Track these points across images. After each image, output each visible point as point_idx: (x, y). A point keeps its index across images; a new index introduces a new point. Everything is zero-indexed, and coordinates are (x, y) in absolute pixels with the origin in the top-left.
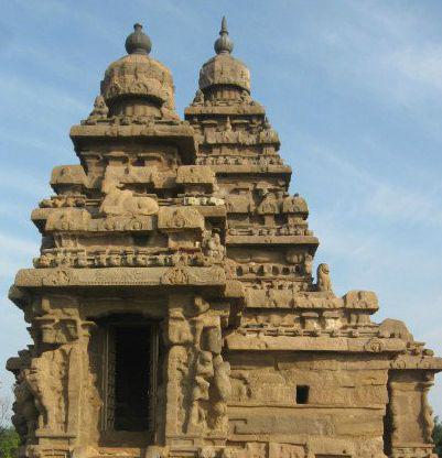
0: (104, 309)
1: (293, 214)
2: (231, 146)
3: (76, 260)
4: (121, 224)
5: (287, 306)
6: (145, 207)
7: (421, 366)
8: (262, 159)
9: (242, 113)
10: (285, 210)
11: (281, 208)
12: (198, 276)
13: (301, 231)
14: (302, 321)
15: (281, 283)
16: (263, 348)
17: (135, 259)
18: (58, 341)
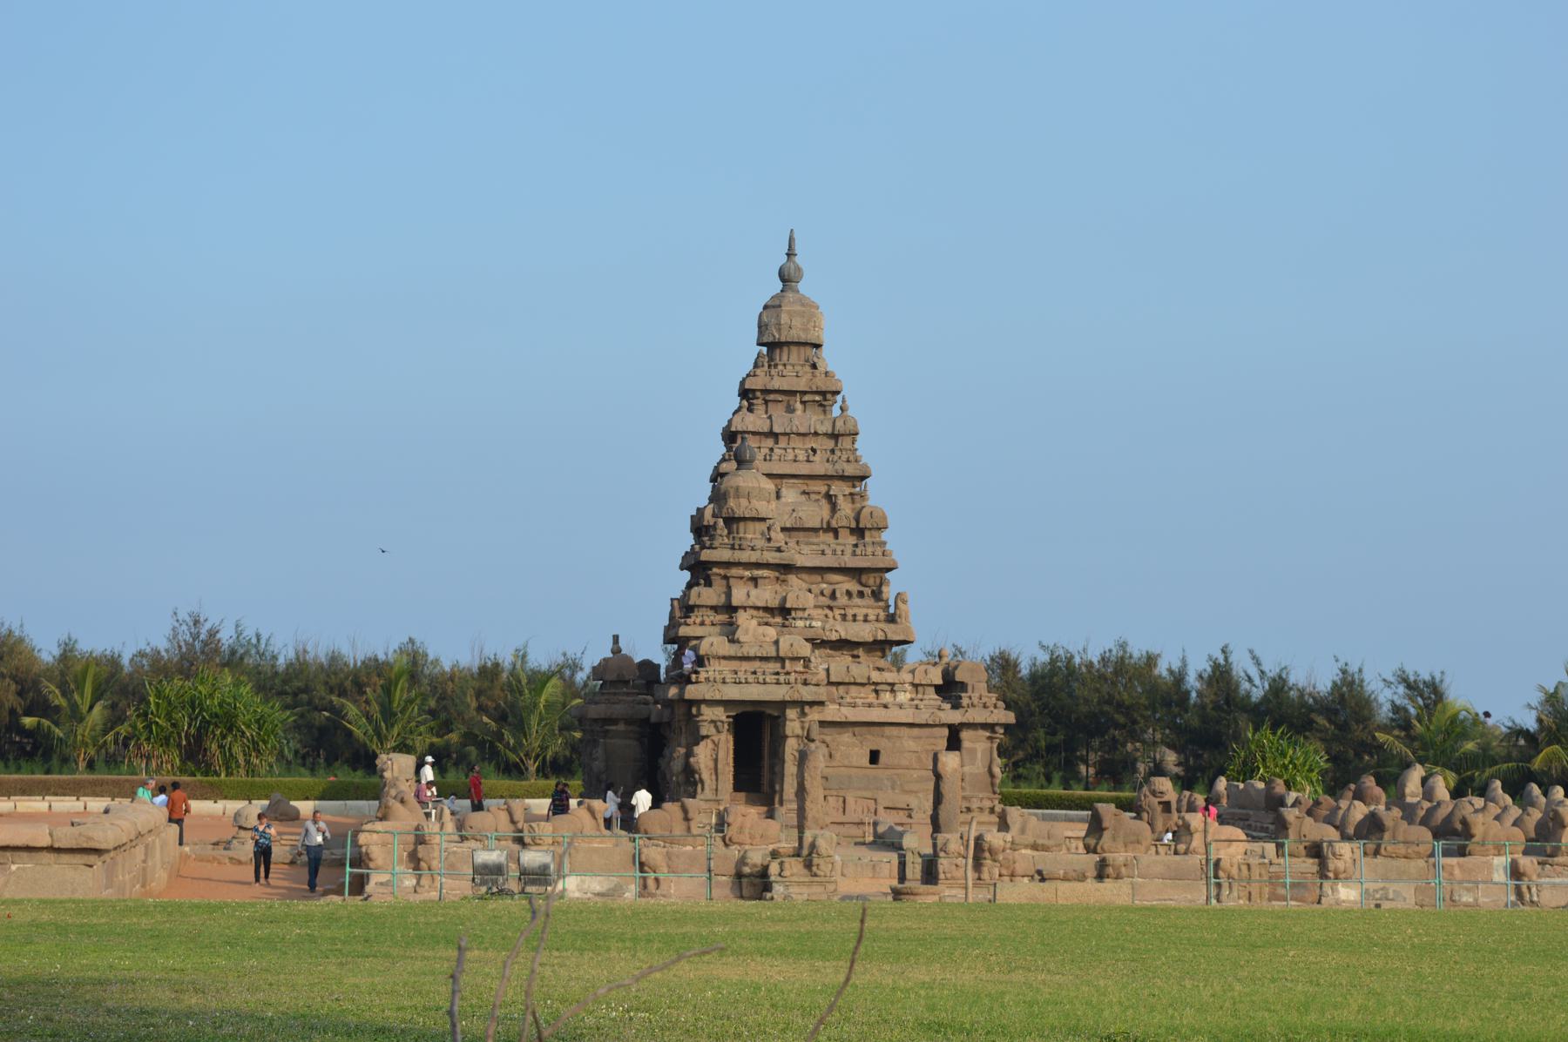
0: (740, 710)
1: (870, 529)
3: (724, 679)
5: (865, 681)
6: (768, 635)
7: (990, 721)
8: (838, 453)
9: (815, 389)
10: (861, 526)
11: (858, 521)
12: (807, 694)
13: (879, 551)
14: (877, 692)
15: (855, 611)
16: (844, 720)
17: (764, 679)
18: (709, 734)
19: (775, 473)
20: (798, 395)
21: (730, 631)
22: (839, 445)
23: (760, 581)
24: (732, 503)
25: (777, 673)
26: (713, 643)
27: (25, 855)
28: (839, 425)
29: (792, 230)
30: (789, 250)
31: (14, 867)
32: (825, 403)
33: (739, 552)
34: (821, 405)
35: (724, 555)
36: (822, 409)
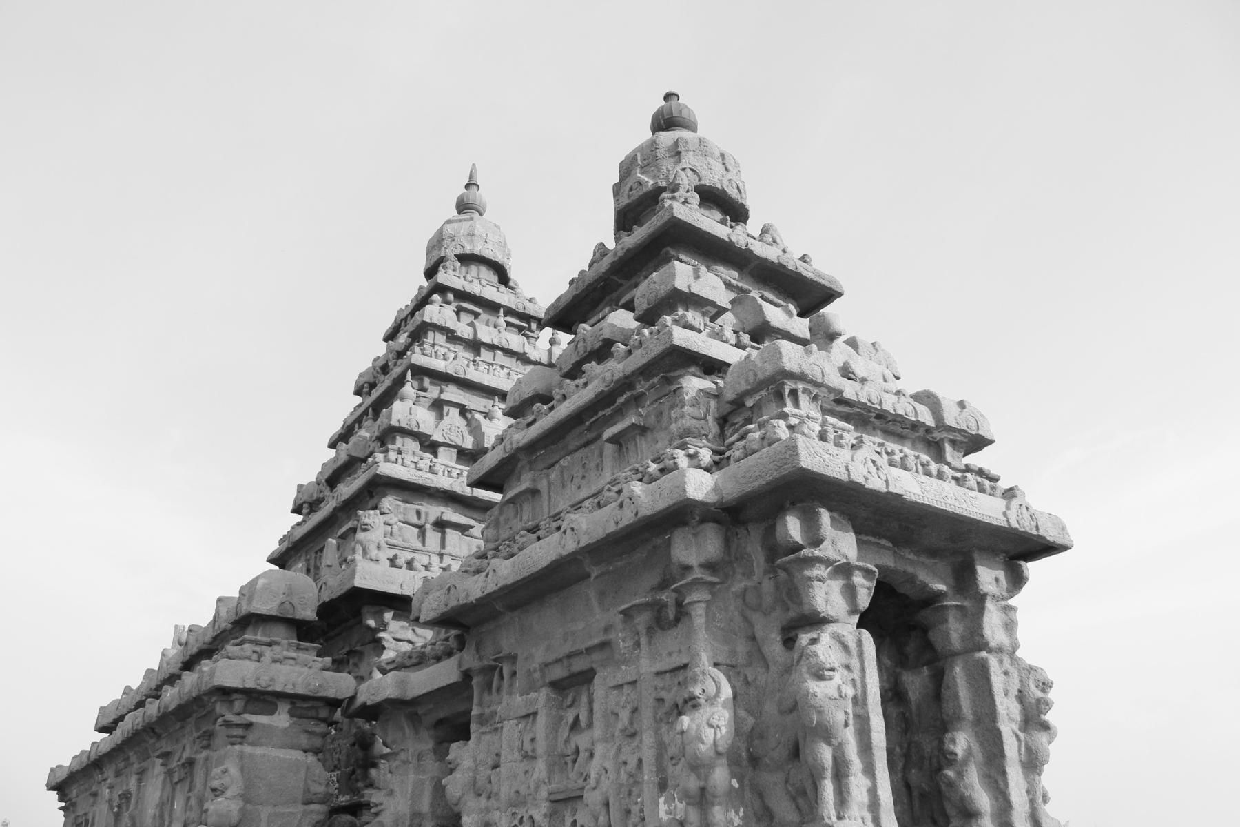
2: (509, 352)
9: (521, 310)
20: (502, 310)
24: (689, 159)
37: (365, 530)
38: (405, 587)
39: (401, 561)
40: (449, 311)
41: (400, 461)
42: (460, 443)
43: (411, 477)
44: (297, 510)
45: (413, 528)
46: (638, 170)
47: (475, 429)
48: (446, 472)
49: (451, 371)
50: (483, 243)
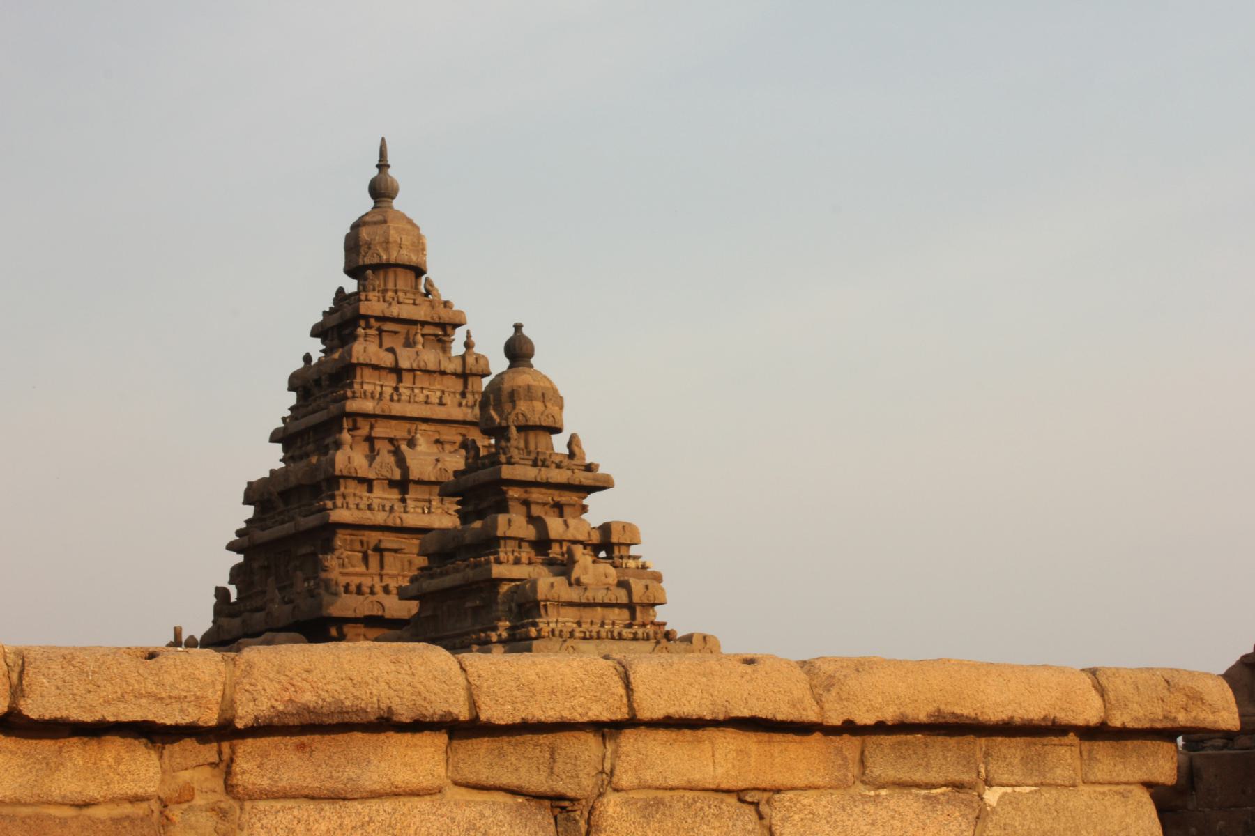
4: (600, 596)
9: (437, 320)
19: (409, 415)
21: (564, 567)
22: (470, 387)
23: (567, 511)
24: (522, 406)
25: (630, 626)
26: (547, 583)
27: (1012, 748)
28: (470, 360)
29: (383, 139)
30: (380, 161)
31: (992, 796)
32: (445, 338)
33: (543, 469)
34: (440, 341)
35: (530, 473)
36: (440, 345)
37: (326, 571)
38: (357, 611)
39: (353, 588)
40: (373, 347)
41: (345, 505)
42: (389, 476)
43: (354, 520)
44: (247, 501)
45: (357, 553)
46: (491, 408)
47: (401, 462)
48: (381, 508)
49: (378, 412)
50: (398, 249)
